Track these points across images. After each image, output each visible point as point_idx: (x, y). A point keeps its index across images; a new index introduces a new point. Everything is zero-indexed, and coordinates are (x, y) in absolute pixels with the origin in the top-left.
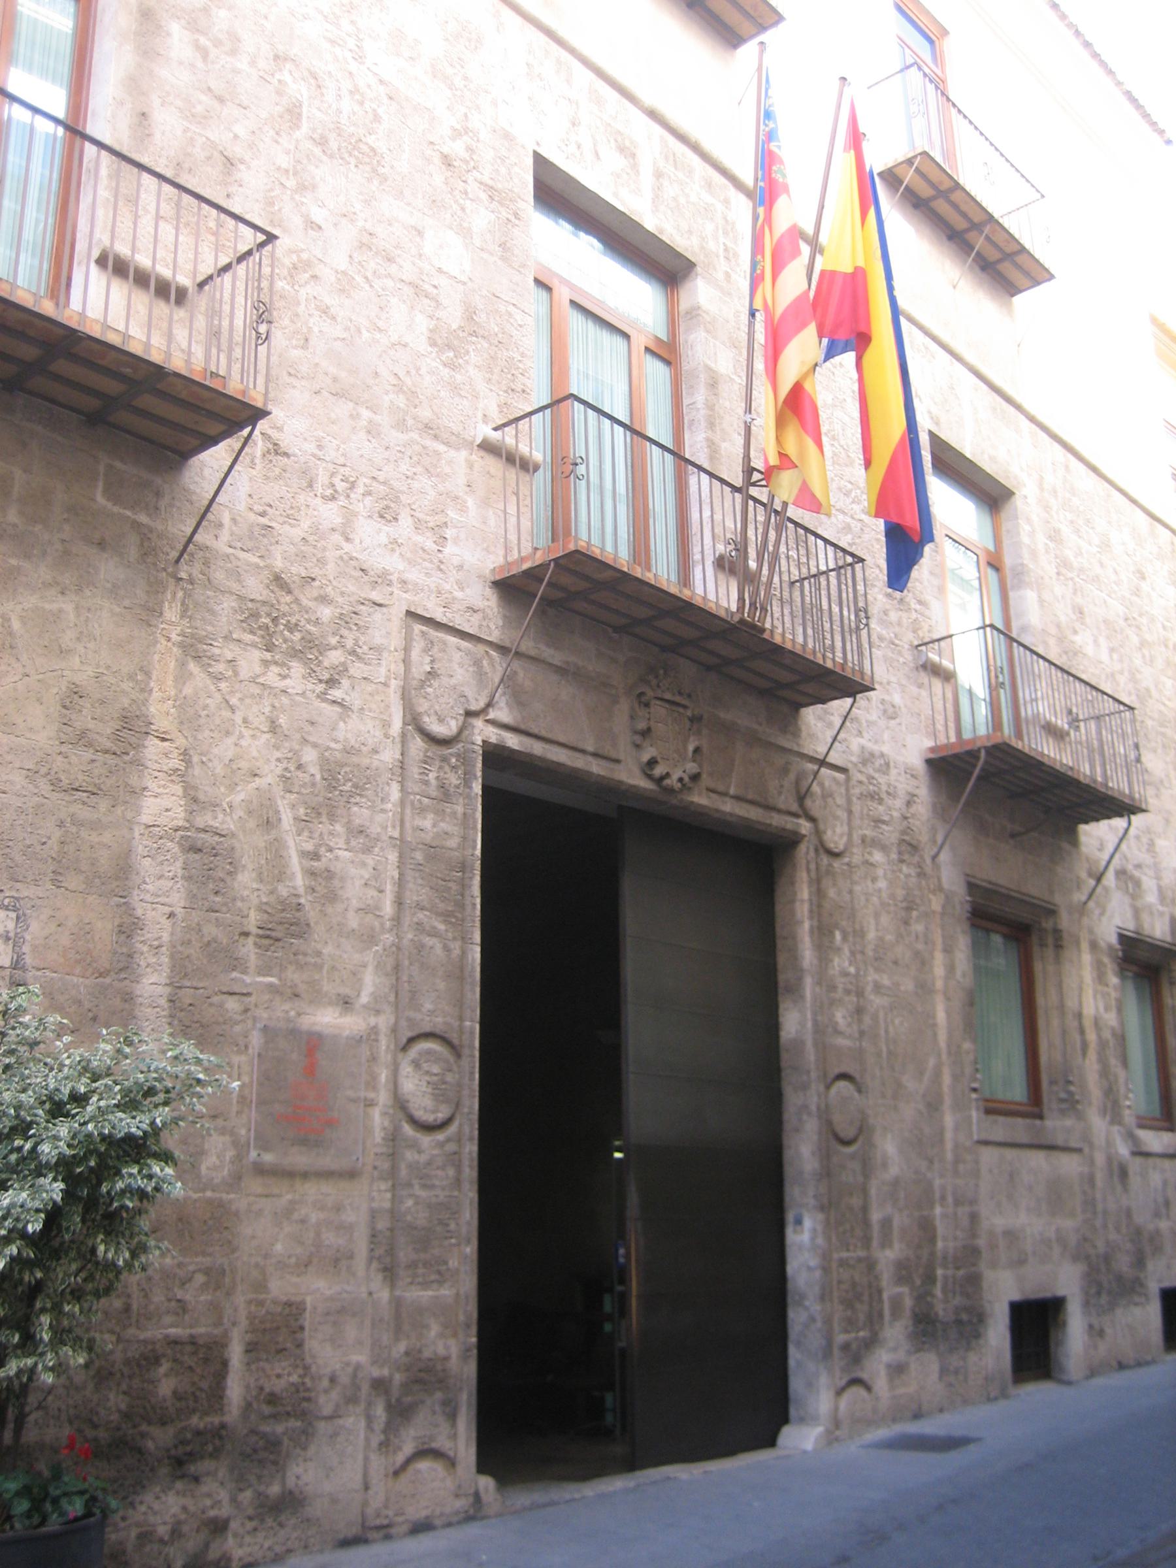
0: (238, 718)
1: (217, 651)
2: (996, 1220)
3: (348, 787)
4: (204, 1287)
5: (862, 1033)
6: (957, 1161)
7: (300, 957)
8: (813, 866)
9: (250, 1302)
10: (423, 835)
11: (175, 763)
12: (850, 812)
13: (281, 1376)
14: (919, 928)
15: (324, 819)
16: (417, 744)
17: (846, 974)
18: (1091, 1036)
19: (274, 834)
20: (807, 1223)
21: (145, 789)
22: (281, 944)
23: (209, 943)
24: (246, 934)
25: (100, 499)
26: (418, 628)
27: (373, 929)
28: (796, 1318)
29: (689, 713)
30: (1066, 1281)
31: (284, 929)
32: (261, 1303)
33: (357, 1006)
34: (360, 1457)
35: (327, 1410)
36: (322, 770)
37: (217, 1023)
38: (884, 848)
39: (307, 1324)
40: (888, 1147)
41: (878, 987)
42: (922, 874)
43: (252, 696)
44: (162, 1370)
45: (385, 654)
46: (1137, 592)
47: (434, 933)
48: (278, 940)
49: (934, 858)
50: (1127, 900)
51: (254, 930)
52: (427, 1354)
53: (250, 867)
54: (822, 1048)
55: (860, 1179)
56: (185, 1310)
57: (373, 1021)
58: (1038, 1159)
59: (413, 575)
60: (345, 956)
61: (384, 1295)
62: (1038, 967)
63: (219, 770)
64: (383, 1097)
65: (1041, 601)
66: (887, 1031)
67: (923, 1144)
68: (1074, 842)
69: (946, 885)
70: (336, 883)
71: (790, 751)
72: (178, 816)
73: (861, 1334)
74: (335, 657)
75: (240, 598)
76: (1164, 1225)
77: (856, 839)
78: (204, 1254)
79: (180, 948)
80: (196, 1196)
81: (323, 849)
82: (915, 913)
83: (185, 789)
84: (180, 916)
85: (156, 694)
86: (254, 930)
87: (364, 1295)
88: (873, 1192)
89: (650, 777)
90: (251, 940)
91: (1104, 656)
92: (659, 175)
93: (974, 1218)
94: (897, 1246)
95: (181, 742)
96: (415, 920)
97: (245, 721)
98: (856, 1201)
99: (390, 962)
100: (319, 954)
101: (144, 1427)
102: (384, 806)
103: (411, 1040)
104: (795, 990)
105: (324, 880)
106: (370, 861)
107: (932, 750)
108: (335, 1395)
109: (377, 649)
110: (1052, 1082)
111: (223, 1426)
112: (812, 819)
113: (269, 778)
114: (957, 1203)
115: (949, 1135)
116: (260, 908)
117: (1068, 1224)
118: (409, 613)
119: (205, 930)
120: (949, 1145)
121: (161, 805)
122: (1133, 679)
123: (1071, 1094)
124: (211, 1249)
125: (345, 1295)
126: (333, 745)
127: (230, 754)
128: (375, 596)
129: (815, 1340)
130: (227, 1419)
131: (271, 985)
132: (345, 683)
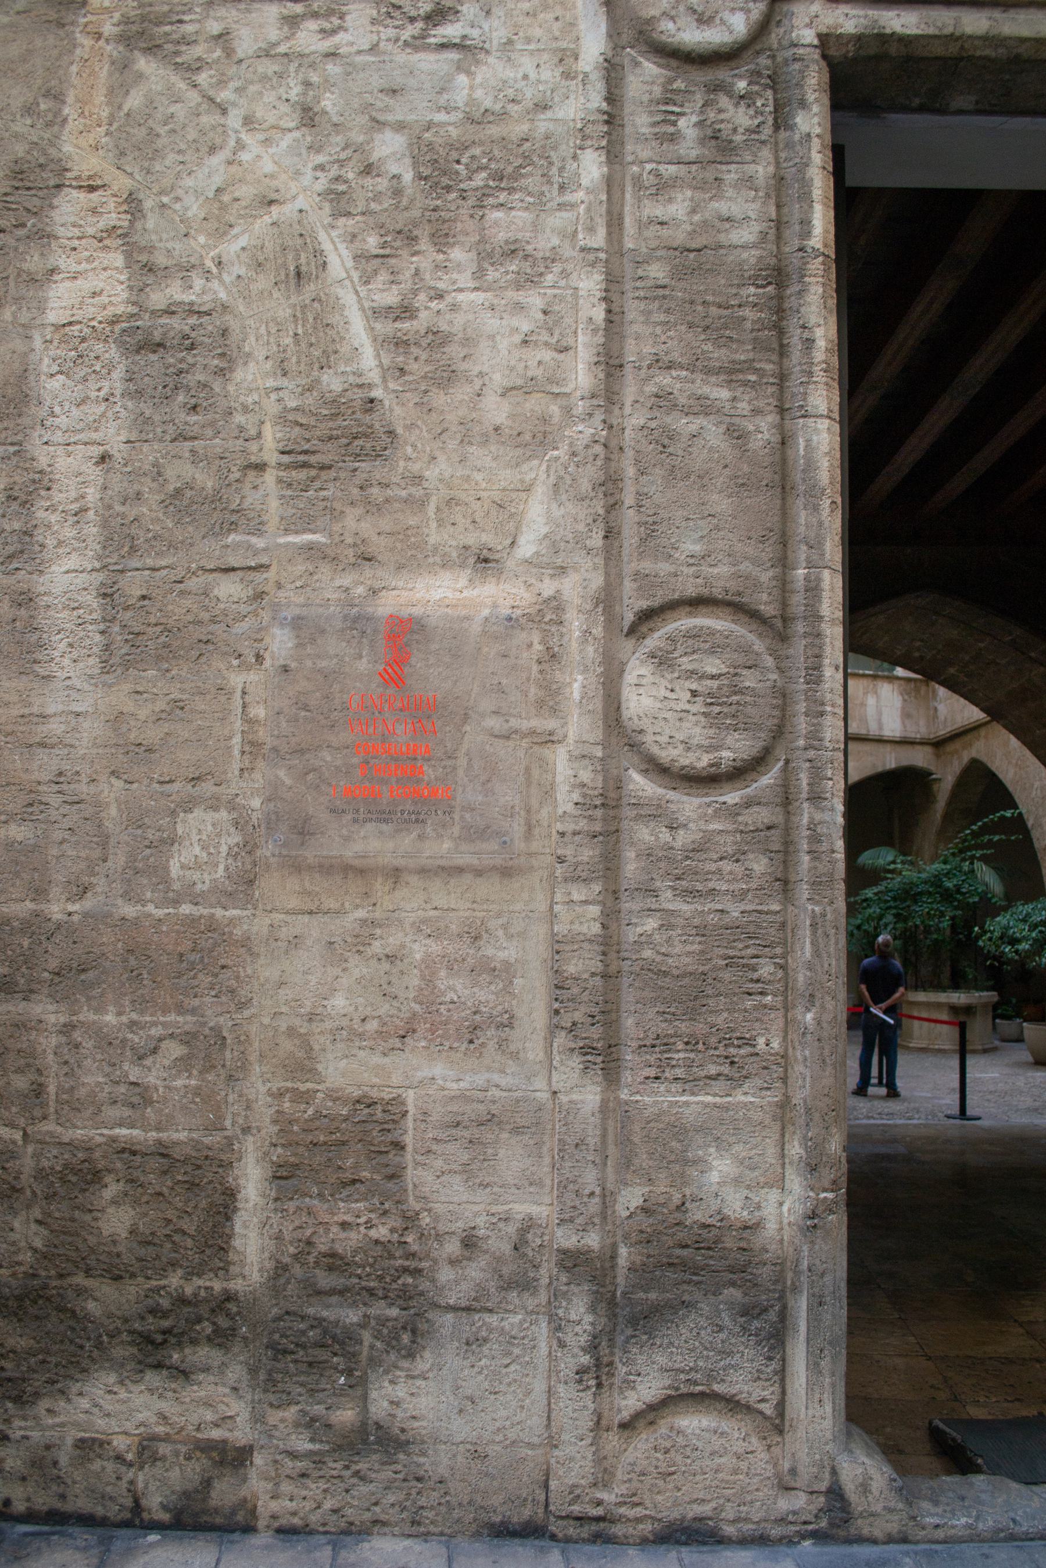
0: (234, 120)
1: (189, 28)
3: (480, 179)
4: (183, 1064)
7: (375, 490)
9: (280, 1094)
10: (665, 232)
11: (111, 218)
13: (351, 1225)
15: (424, 245)
19: (310, 289)
21: (53, 271)
22: (332, 474)
23: (178, 493)
24: (260, 467)
27: (545, 420)
32: (304, 1098)
33: (510, 564)
34: (539, 1386)
36: (415, 164)
37: (200, 623)
39: (408, 1140)
43: (265, 78)
44: (108, 1193)
47: (704, 407)
48: (323, 467)
51: (271, 457)
52: (697, 1215)
53: (260, 353)
56: (148, 1102)
57: (548, 588)
60: (478, 477)
61: (590, 1096)
63: (195, 209)
64: (579, 726)
70: (455, 350)
72: (116, 296)
78: (180, 1009)
79: (119, 508)
80: (160, 913)
81: (422, 297)
83: (128, 256)
86: (271, 457)
87: (544, 1096)
90: (270, 477)
95: (121, 183)
96: (650, 389)
97: (248, 121)
99: (589, 475)
100: (418, 479)
101: (79, 1279)
102: (568, 197)
103: (648, 616)
105: (424, 351)
106: (535, 300)
108: (475, 1271)
111: (229, 1297)
116: (282, 419)
119: (170, 473)
124: (196, 1002)
125: (494, 1092)
126: (441, 117)
127: (217, 181)
130: (237, 1285)
131: (310, 547)
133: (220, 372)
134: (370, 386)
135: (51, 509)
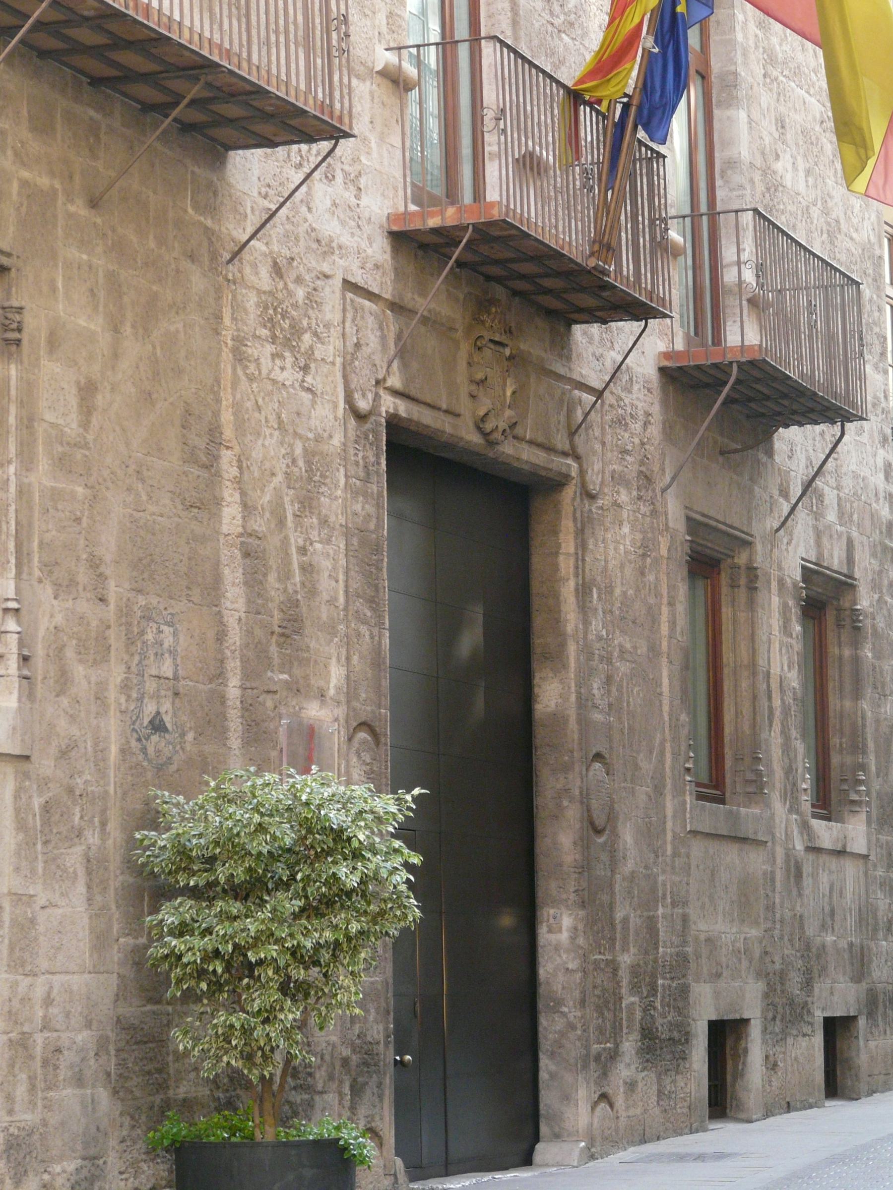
2: (703, 926)
5: (610, 705)
6: (675, 855)
8: (578, 515)
12: (603, 444)
14: (651, 578)
16: (352, 422)
17: (600, 638)
18: (777, 703)
20: (567, 921)
25: (190, 210)
26: (349, 295)
28: (549, 1026)
29: (507, 352)
30: (751, 1003)
31: (291, 628)
35: (320, 1087)
38: (627, 484)
40: (627, 836)
41: (622, 651)
42: (654, 513)
45: (332, 330)
47: (364, 622)
49: (664, 491)
50: (810, 521)
51: (277, 630)
53: (274, 567)
54: (584, 722)
55: (609, 874)
58: (731, 854)
59: (345, 239)
62: (726, 612)
65: (750, 121)
66: (628, 702)
67: (651, 834)
68: (770, 453)
69: (671, 525)
71: (559, 377)
73: (608, 1045)
74: (307, 338)
75: (259, 292)
76: (830, 939)
77: (608, 476)
82: (649, 560)
84: (244, 620)
85: (224, 403)
88: (617, 888)
89: (479, 429)
90: (274, 638)
91: (801, 187)
93: (685, 919)
94: (632, 950)
97: (267, 421)
98: (605, 898)
104: (557, 658)
107: (667, 355)
109: (327, 326)
110: (738, 759)
112: (577, 458)
113: (280, 477)
114: (674, 904)
115: (669, 824)
117: (754, 933)
118: (345, 282)
120: (669, 836)
122: (826, 212)
123: (759, 774)
128: (326, 268)
129: (573, 1049)
131: (286, 682)
132: (312, 365)
133: (265, 575)
134: (296, 592)
135: (227, 648)
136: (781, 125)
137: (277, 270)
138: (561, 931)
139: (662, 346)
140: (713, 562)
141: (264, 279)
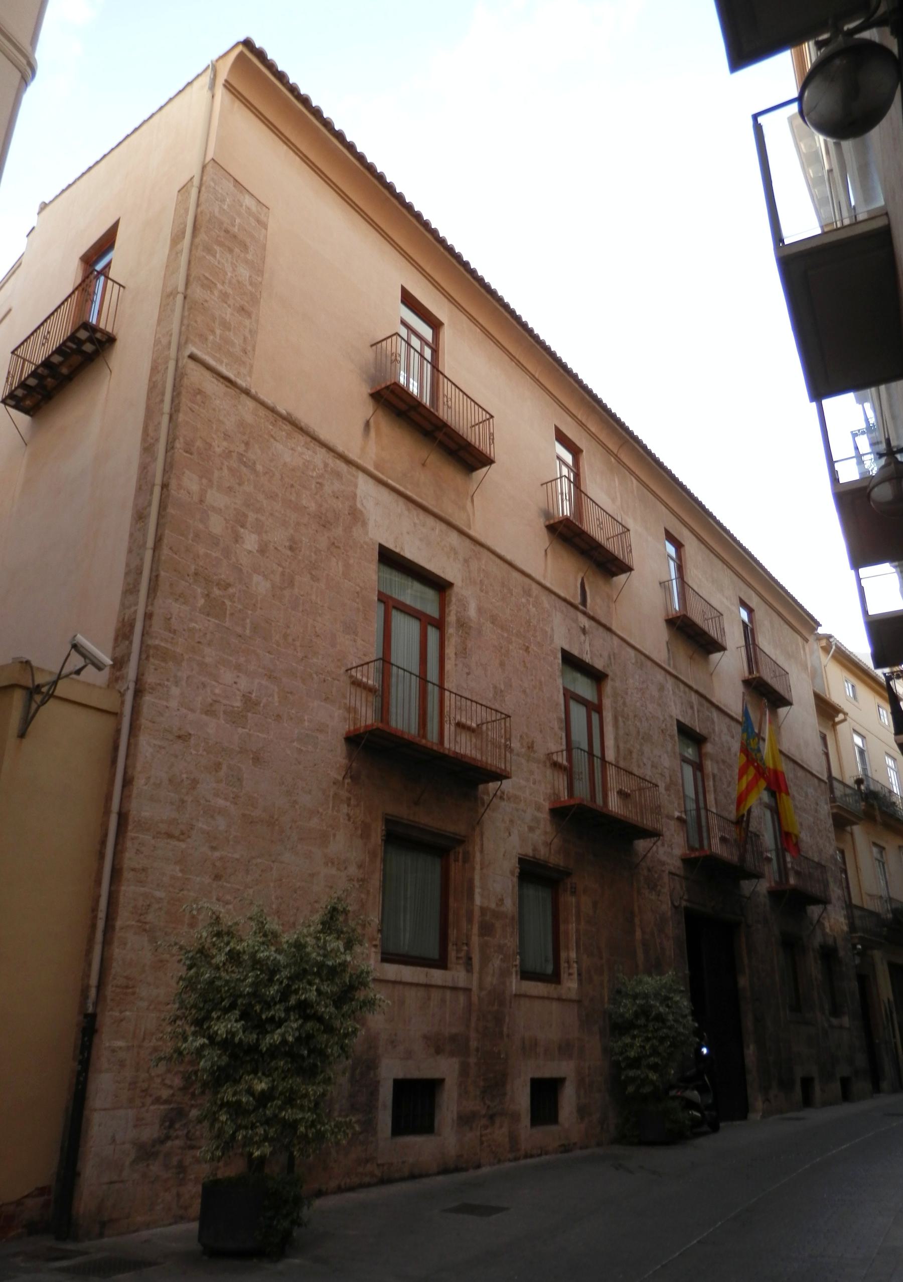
46: (816, 811)
74: (659, 887)
92: (698, 711)
121: (638, 934)
136: (801, 824)
137: (649, 870)
138: (751, 1051)
139: (768, 885)
140: (792, 945)
141: (645, 872)
